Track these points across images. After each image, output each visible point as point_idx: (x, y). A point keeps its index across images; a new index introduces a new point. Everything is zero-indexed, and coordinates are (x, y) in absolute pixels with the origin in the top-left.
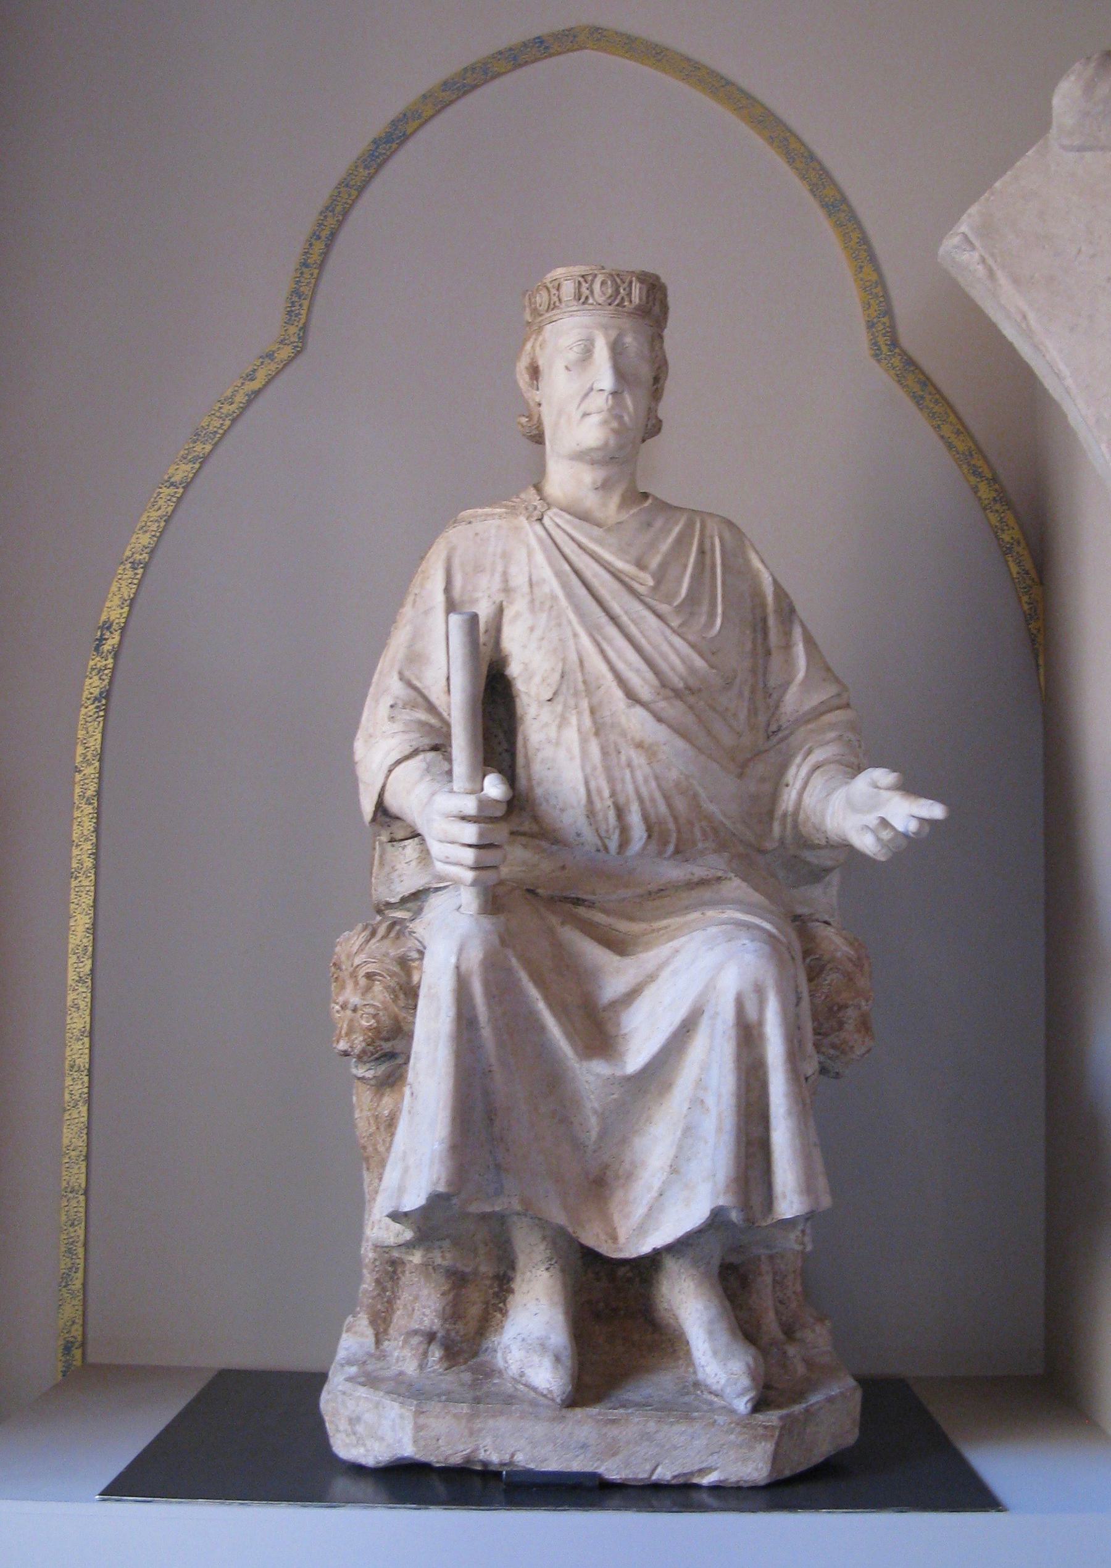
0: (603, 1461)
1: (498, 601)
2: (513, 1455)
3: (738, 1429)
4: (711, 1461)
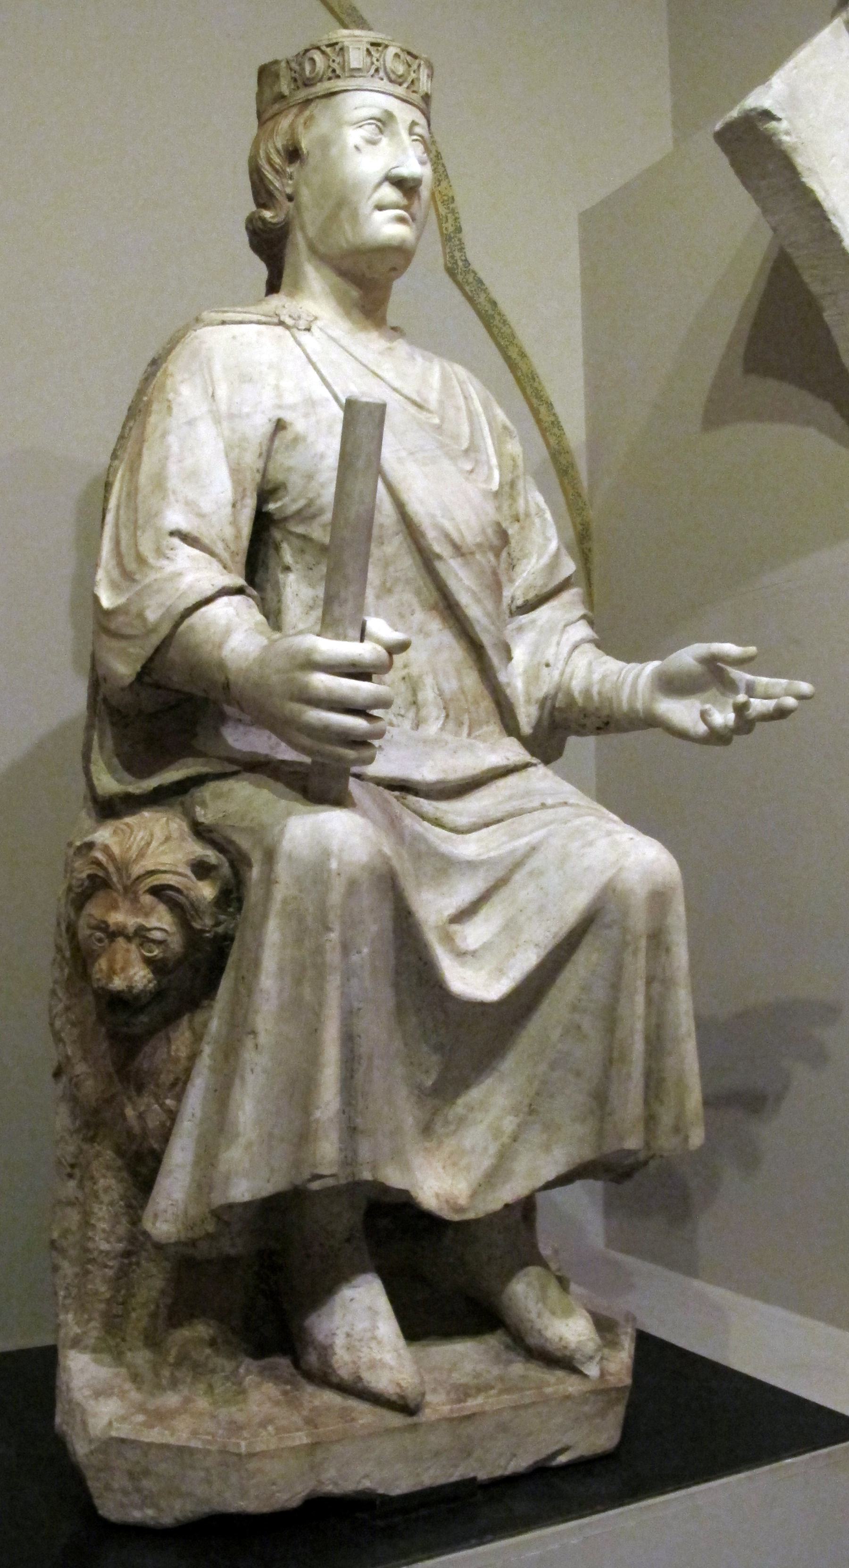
0: (456, 1466)
1: (274, 419)
2: (359, 1482)
3: (592, 1398)
4: (566, 1440)
